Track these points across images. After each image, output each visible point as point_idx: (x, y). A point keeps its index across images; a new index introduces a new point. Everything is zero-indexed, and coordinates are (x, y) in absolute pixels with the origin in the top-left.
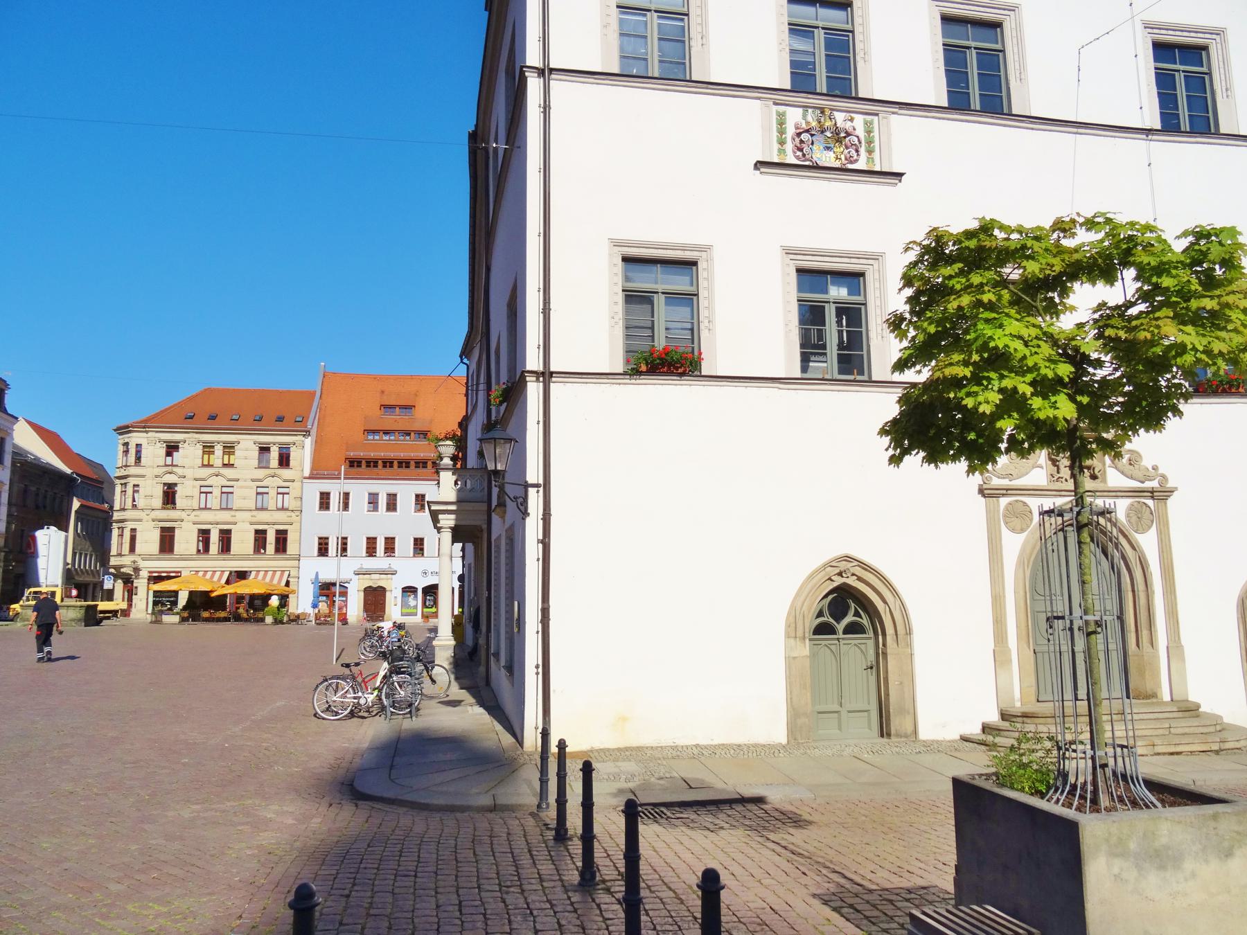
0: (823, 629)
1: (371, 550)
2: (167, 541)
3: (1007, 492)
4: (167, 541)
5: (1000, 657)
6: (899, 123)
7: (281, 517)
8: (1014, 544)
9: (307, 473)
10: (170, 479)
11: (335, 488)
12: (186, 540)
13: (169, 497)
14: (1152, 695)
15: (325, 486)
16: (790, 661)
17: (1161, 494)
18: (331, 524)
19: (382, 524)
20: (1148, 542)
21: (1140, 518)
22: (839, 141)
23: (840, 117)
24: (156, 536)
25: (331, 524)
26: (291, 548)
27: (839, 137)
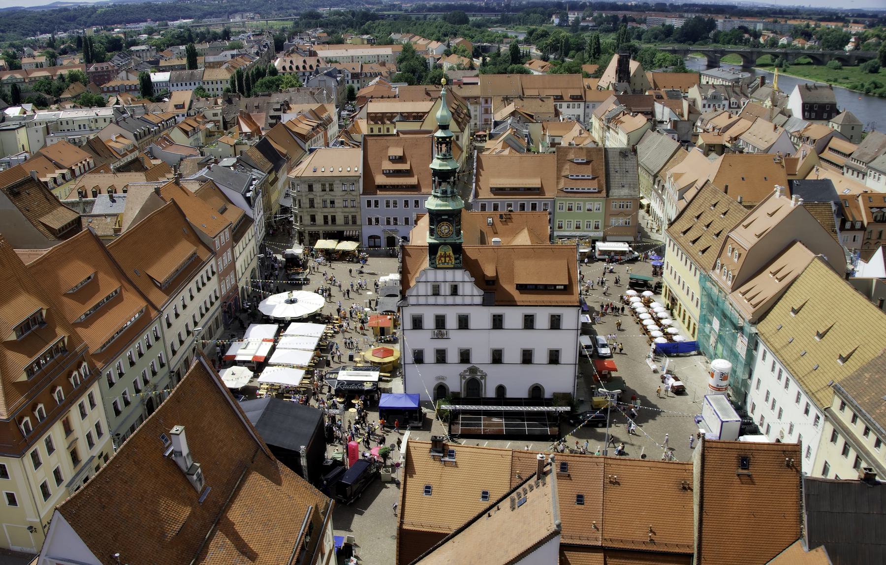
1: (388, 223)
2: (313, 218)
4: (313, 218)
7: (353, 210)
8: (463, 381)
9: (361, 192)
10: (311, 196)
11: (372, 198)
12: (320, 219)
13: (312, 205)
15: (369, 197)
18: (373, 212)
19: (392, 212)
20: (483, 381)
21: (482, 378)
24: (309, 218)
25: (373, 212)
26: (358, 222)
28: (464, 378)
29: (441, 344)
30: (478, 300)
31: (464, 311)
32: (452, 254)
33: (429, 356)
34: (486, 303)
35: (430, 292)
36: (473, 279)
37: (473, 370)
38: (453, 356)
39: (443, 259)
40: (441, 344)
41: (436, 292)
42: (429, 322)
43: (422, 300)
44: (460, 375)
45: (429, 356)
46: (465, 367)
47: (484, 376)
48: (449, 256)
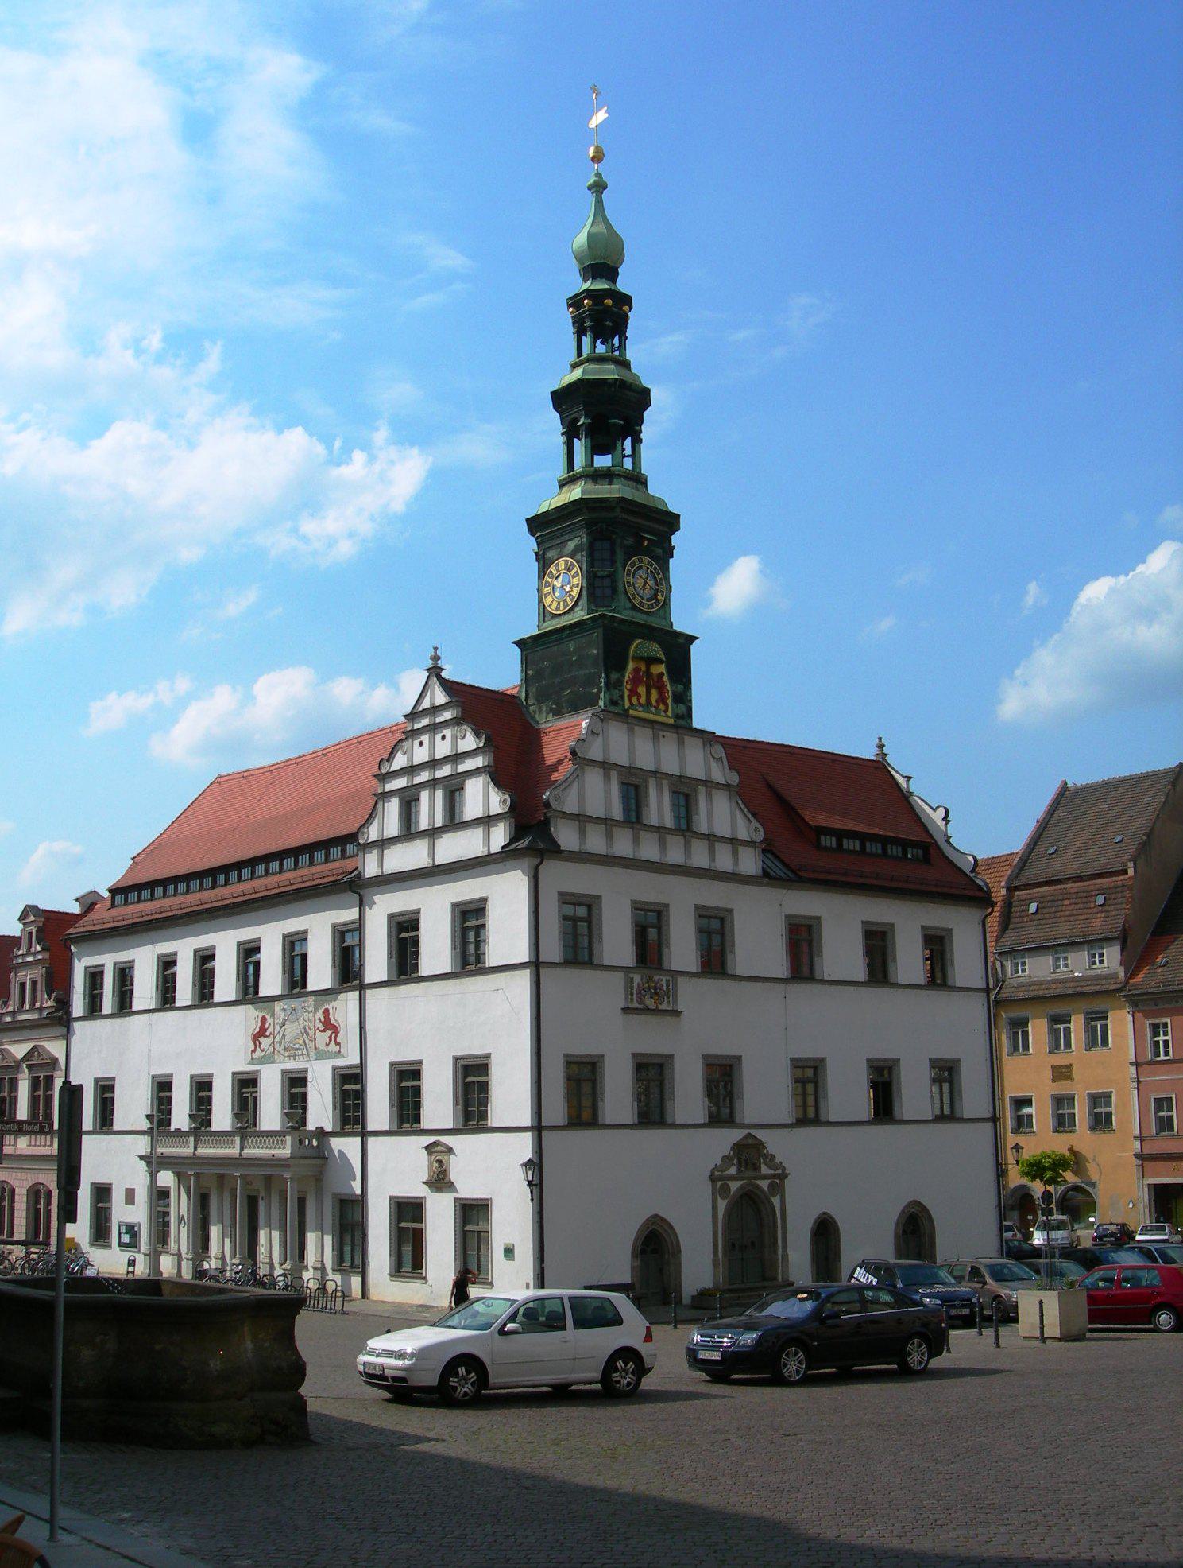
0: (643, 1252)
3: (721, 1178)
5: (715, 1264)
6: (681, 980)
8: (722, 1205)
14: (775, 1279)
16: (633, 1269)
17: (783, 1176)
20: (776, 1201)
22: (656, 993)
23: (656, 978)
27: (656, 992)
28: (725, 1189)
29: (652, 1038)
30: (750, 863)
31: (715, 895)
32: (665, 679)
33: (618, 1095)
34: (767, 878)
35: (617, 813)
36: (734, 779)
37: (749, 1154)
38: (688, 1095)
39: (642, 690)
40: (652, 1038)
41: (634, 818)
42: (617, 942)
43: (596, 843)
44: (713, 1179)
45: (618, 1095)
46: (725, 1139)
47: (779, 1179)
48: (661, 689)
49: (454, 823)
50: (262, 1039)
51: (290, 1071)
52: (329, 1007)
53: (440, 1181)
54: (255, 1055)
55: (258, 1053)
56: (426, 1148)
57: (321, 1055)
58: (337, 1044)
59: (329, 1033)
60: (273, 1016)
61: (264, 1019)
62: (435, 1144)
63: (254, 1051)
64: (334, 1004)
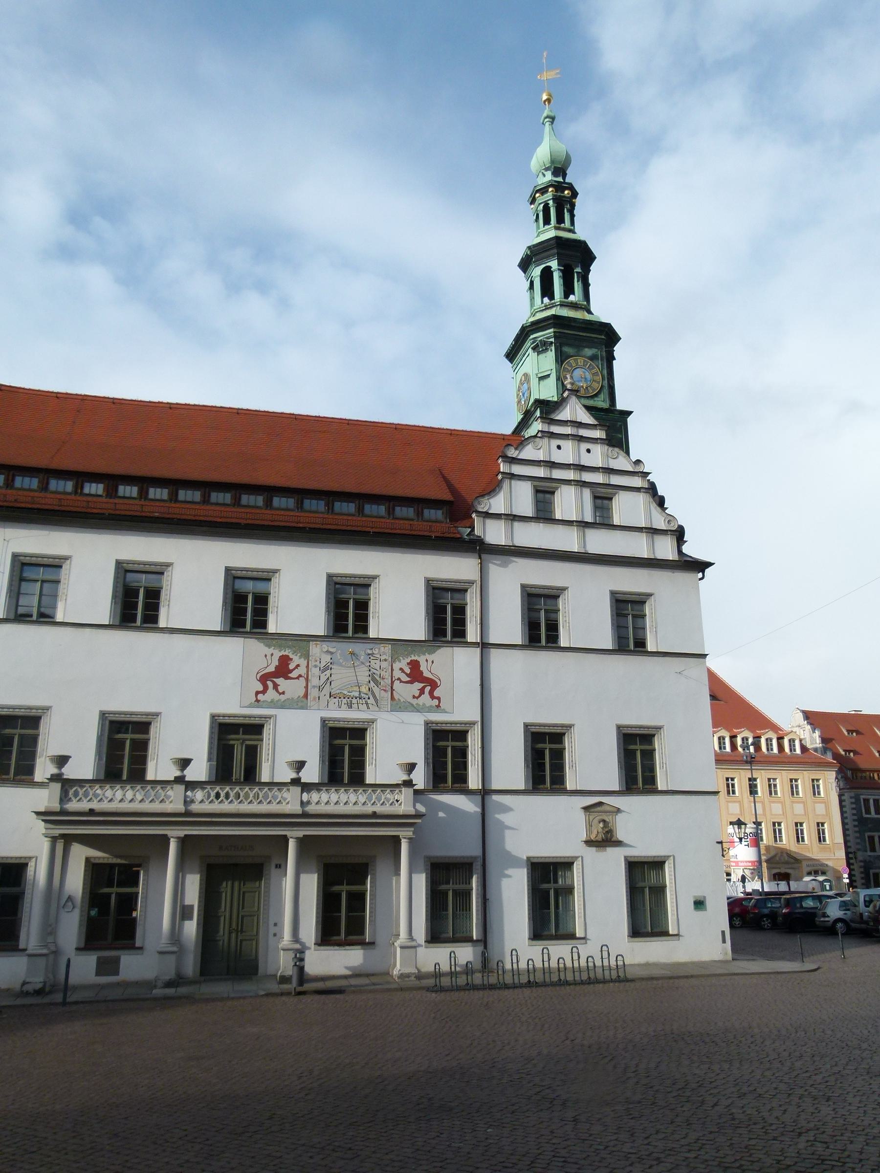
49: (603, 520)
50: (280, 681)
51: (339, 720)
52: (422, 659)
53: (606, 840)
54: (260, 696)
55: (271, 694)
56: (586, 809)
57: (397, 706)
58: (433, 697)
59: (418, 685)
60: (307, 656)
61: (284, 661)
62: (600, 804)
63: (264, 692)
64: (430, 657)
